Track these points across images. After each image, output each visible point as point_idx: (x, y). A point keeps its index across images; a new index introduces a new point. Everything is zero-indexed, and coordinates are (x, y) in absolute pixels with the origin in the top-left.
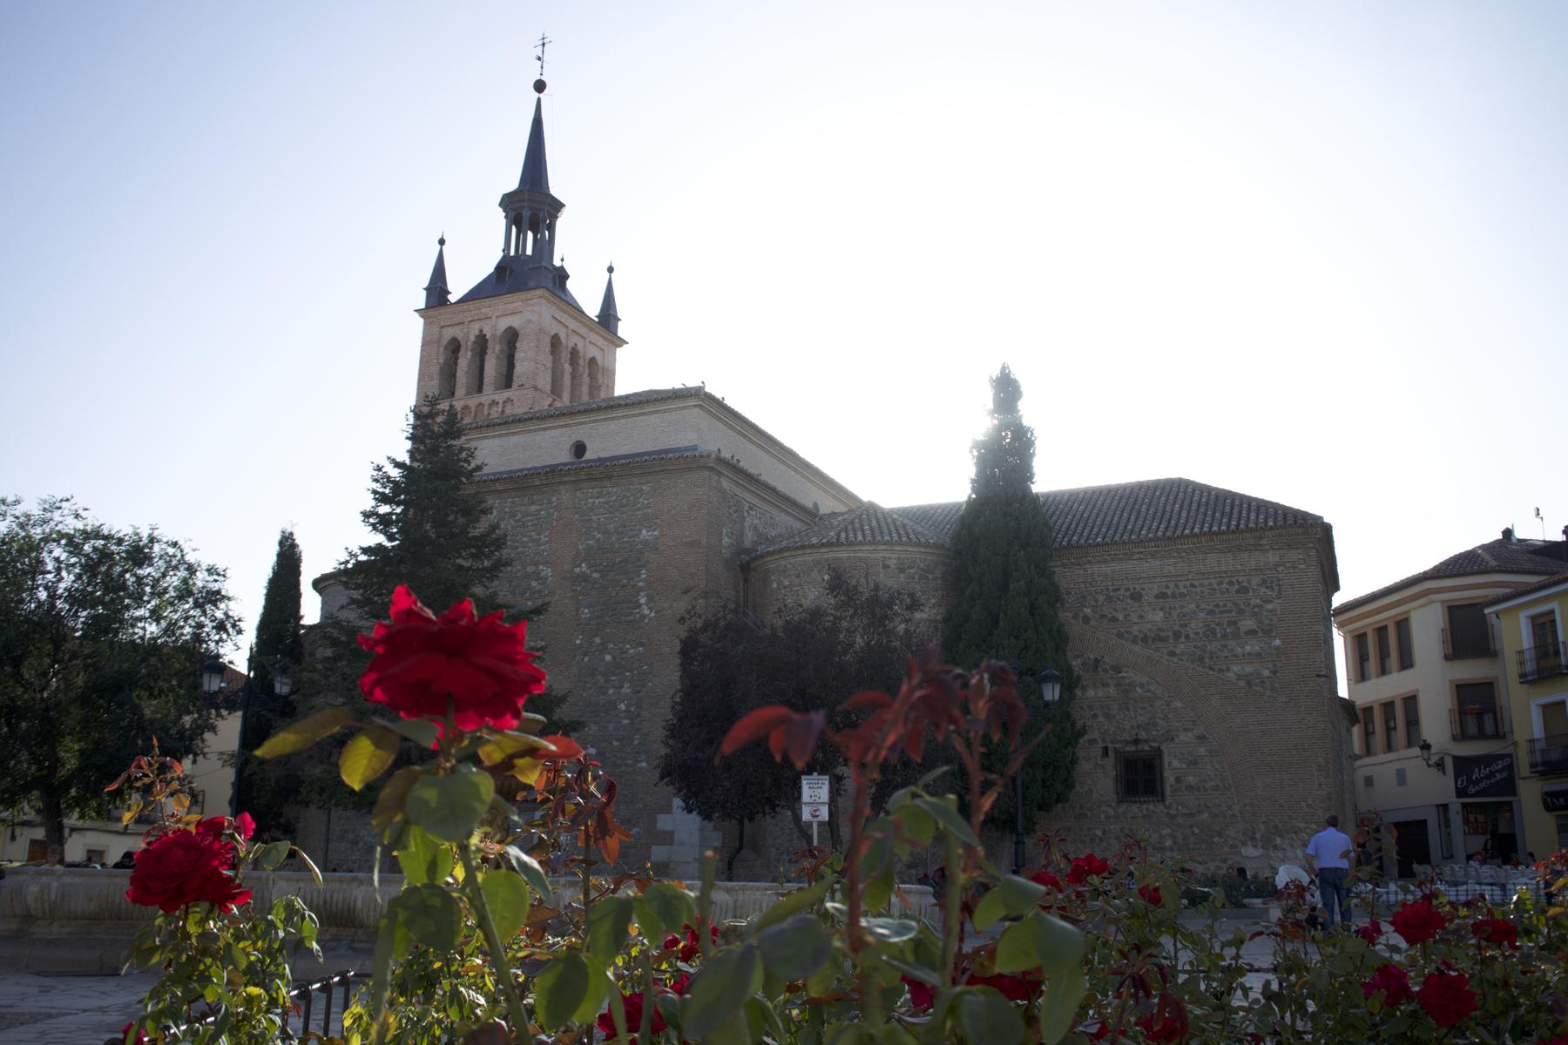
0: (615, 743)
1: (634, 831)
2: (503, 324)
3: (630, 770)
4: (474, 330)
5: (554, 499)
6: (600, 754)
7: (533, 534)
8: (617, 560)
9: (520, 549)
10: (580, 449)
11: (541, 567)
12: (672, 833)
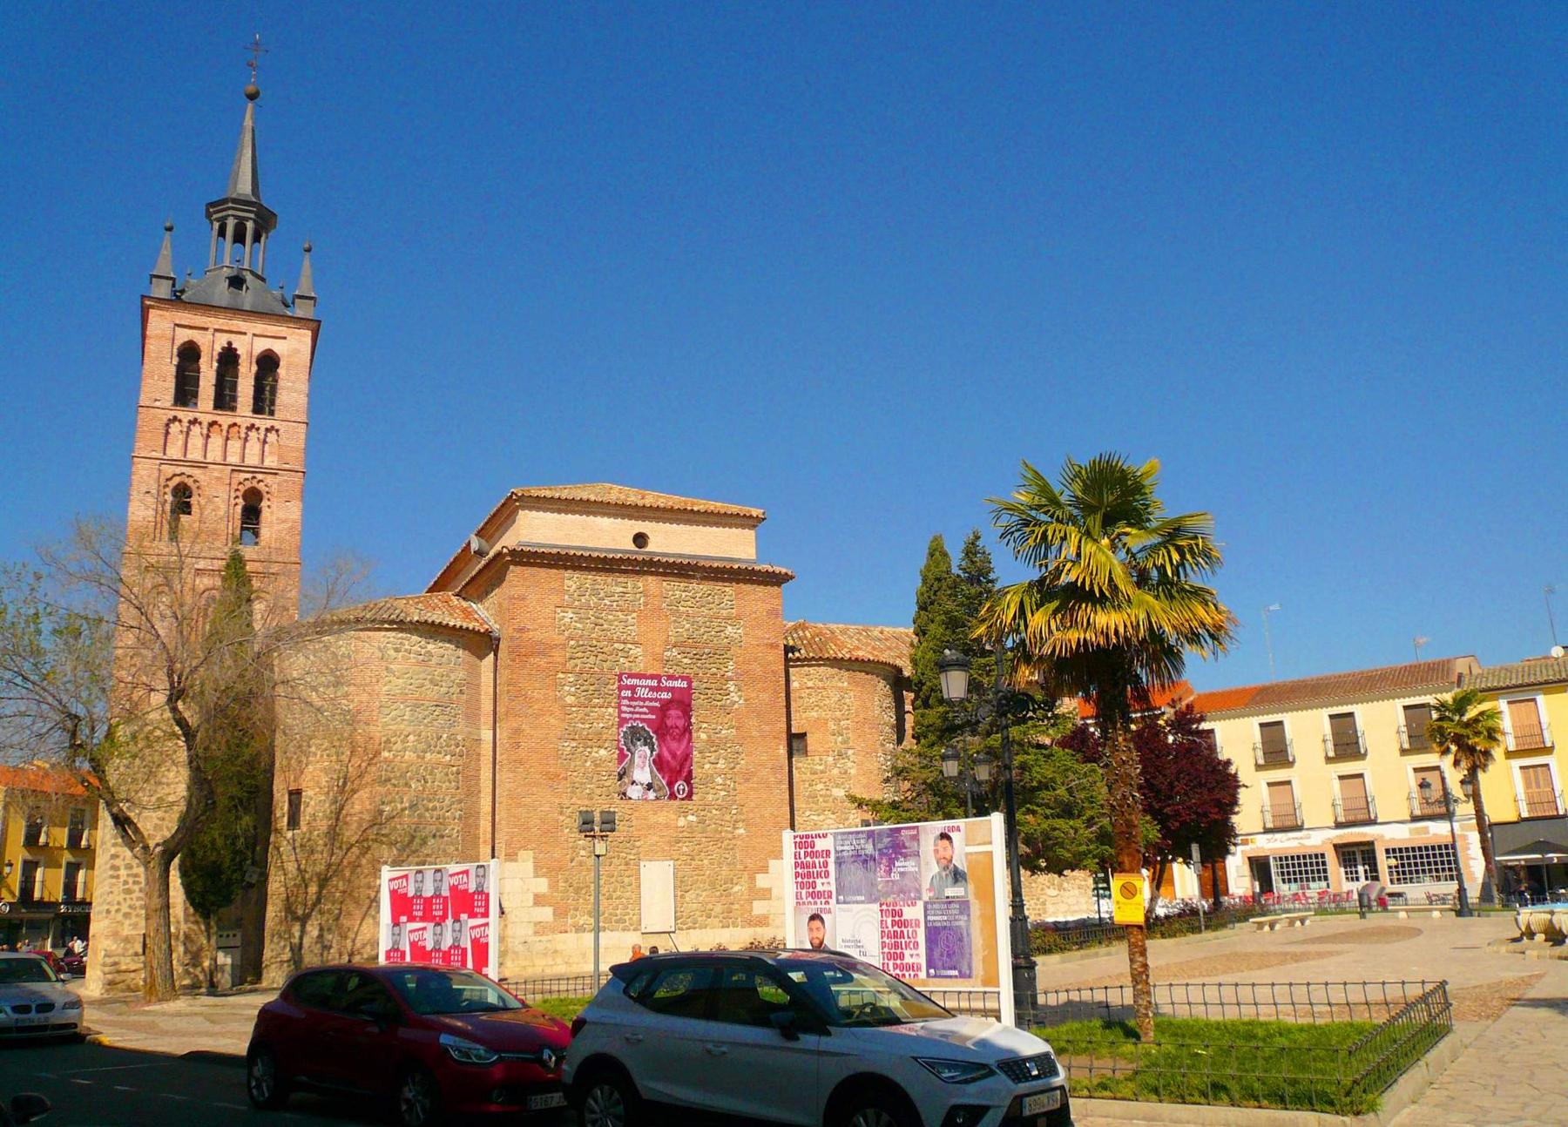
0: (714, 812)
1: (737, 888)
2: (261, 345)
3: (730, 836)
4: (222, 341)
5: (640, 584)
6: (701, 822)
7: (619, 613)
8: (706, 651)
9: (605, 626)
10: (640, 539)
11: (630, 646)
12: (770, 890)
